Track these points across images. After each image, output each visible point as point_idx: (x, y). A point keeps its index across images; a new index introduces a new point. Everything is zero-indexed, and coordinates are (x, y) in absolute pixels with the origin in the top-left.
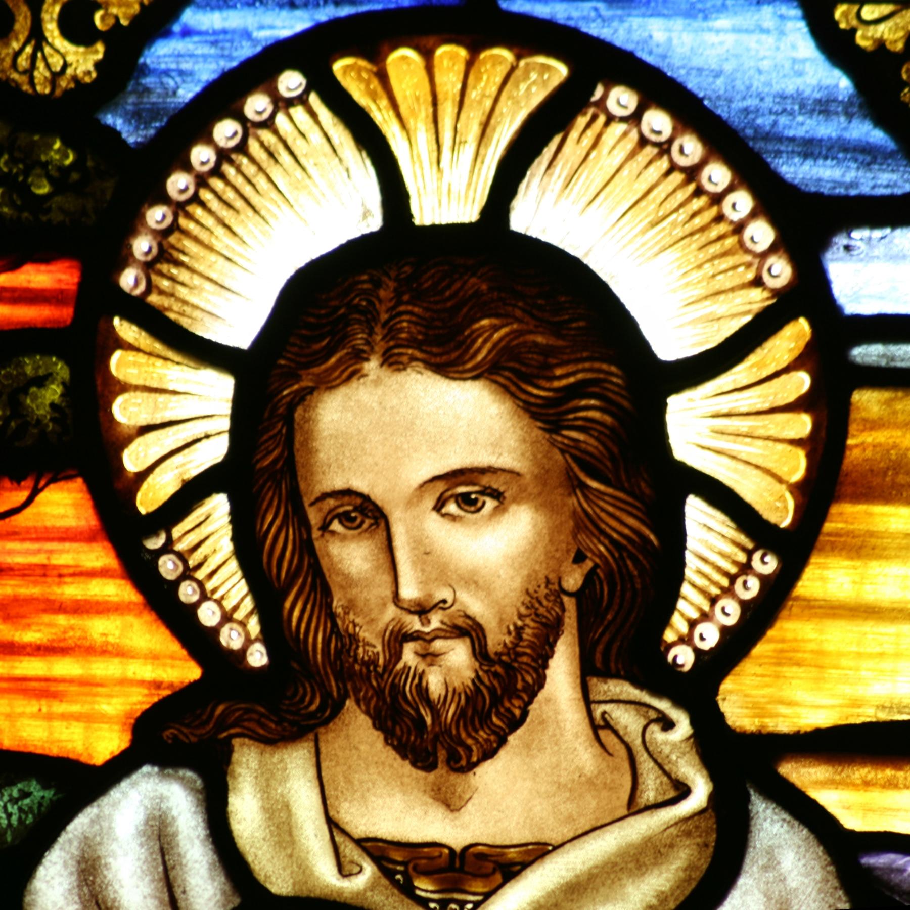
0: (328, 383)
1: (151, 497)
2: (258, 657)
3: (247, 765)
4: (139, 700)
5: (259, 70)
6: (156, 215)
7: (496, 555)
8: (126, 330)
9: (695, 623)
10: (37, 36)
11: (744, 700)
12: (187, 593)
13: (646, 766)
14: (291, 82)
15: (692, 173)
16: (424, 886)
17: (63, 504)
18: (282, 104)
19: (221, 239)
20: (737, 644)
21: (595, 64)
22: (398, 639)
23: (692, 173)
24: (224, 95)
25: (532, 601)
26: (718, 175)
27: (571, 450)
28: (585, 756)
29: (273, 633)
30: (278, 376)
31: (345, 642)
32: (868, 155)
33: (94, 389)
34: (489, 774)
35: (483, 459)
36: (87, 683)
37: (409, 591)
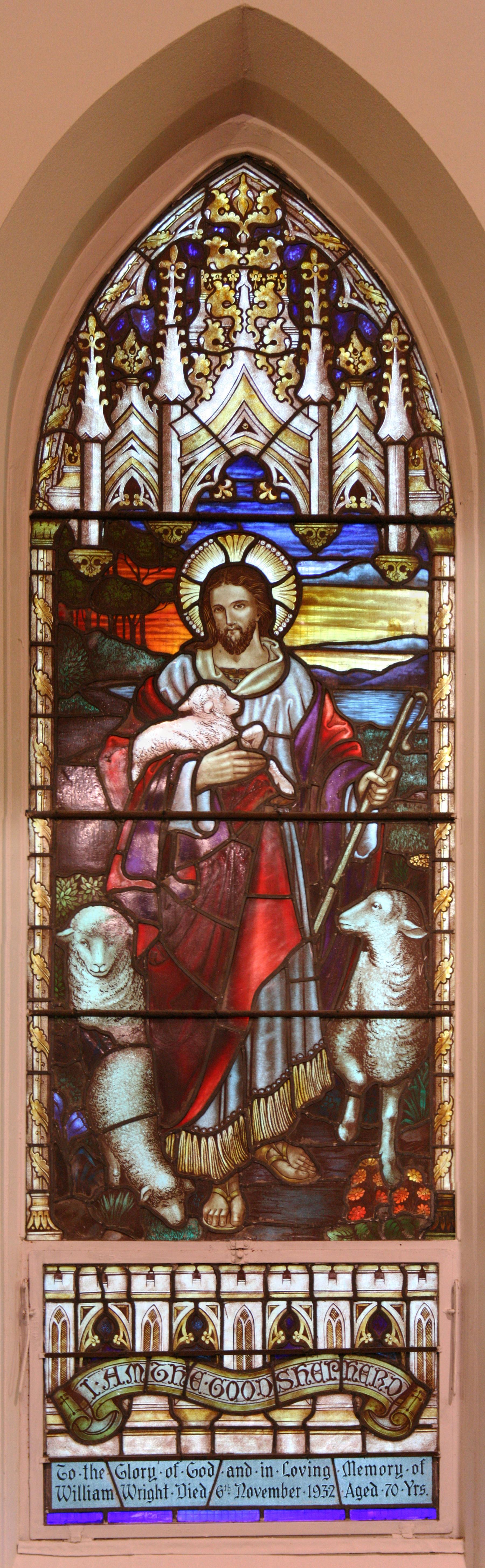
0: (216, 587)
1: (185, 607)
2: (202, 634)
3: (200, 653)
4: (182, 642)
5: (206, 539)
6: (189, 561)
7: (244, 614)
8: (183, 579)
9: (279, 627)
10: (172, 534)
11: (288, 640)
12: (191, 623)
13: (271, 653)
14: (211, 541)
15: (274, 553)
16: (231, 677)
17: (171, 607)
18: (210, 544)
19: (199, 564)
20: (286, 630)
21: (258, 538)
22: (227, 630)
23: (274, 553)
24: (201, 543)
25: (250, 623)
26: (279, 553)
27: (256, 598)
28: (260, 651)
29: (205, 630)
30: (207, 587)
31: (217, 631)
32: (302, 550)
33: (177, 588)
34: (243, 655)
35: (241, 599)
36: (172, 639)
37: (229, 622)
